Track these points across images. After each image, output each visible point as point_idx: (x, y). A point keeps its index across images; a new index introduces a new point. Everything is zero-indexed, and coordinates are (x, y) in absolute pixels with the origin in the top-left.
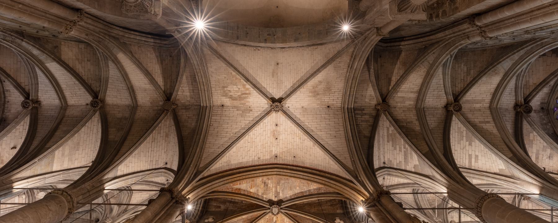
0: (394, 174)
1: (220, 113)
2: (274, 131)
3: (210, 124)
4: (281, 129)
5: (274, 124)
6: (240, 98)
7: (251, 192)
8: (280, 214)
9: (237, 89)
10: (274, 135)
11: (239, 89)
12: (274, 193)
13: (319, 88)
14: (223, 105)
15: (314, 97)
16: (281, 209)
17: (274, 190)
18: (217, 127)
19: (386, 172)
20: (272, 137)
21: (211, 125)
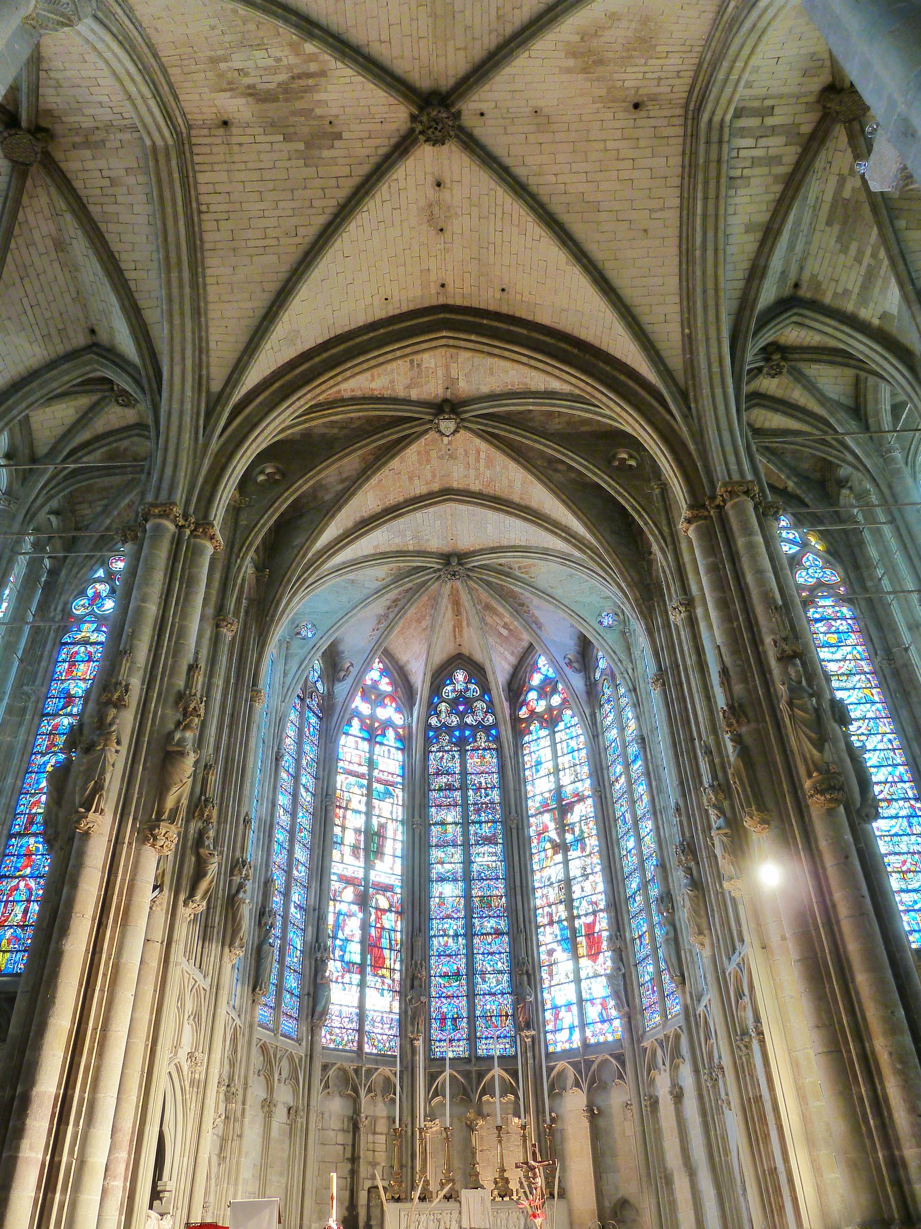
0: (817, 325)
1: (221, 158)
2: (430, 205)
3: (199, 204)
4: (455, 196)
5: (430, 180)
6: (286, 91)
7: (372, 390)
8: (462, 431)
9: (271, 62)
10: (431, 219)
11: (278, 60)
12: (440, 382)
13: (602, 39)
14: (225, 123)
15: (585, 70)
16: (463, 420)
17: (440, 373)
18: (225, 216)
19: (794, 319)
20: (424, 227)
21: (204, 208)
